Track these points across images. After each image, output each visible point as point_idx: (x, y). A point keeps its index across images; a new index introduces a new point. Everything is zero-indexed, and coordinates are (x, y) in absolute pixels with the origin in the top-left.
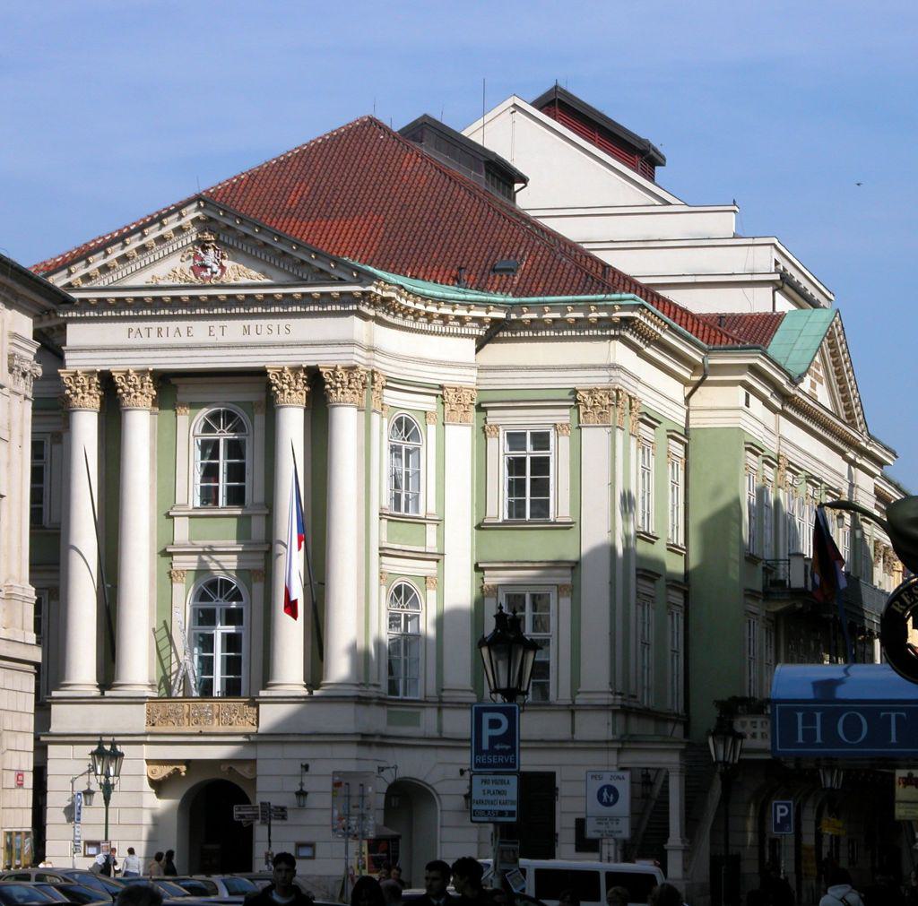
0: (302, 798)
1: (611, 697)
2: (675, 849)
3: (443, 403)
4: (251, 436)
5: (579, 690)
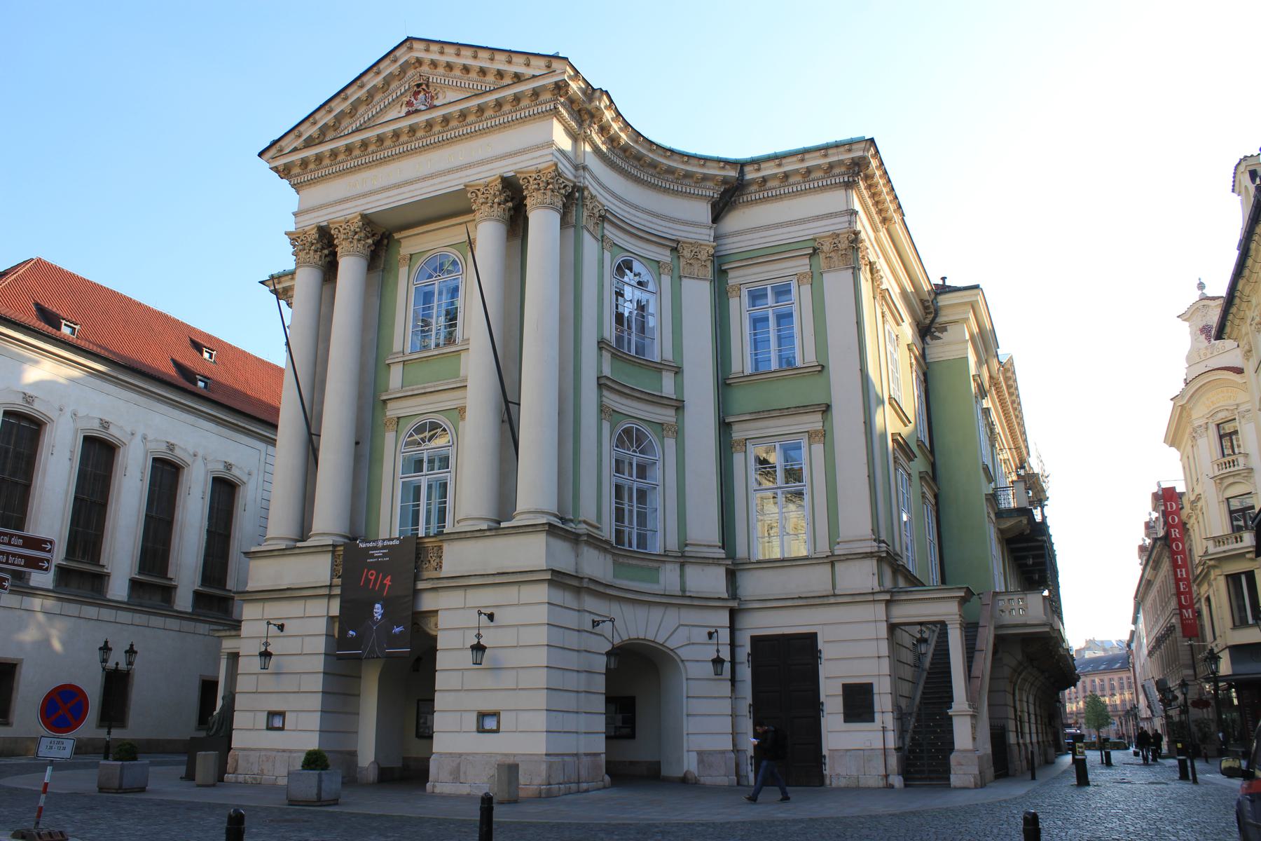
0: (480, 653)
1: (875, 544)
4: (464, 276)
5: (838, 540)
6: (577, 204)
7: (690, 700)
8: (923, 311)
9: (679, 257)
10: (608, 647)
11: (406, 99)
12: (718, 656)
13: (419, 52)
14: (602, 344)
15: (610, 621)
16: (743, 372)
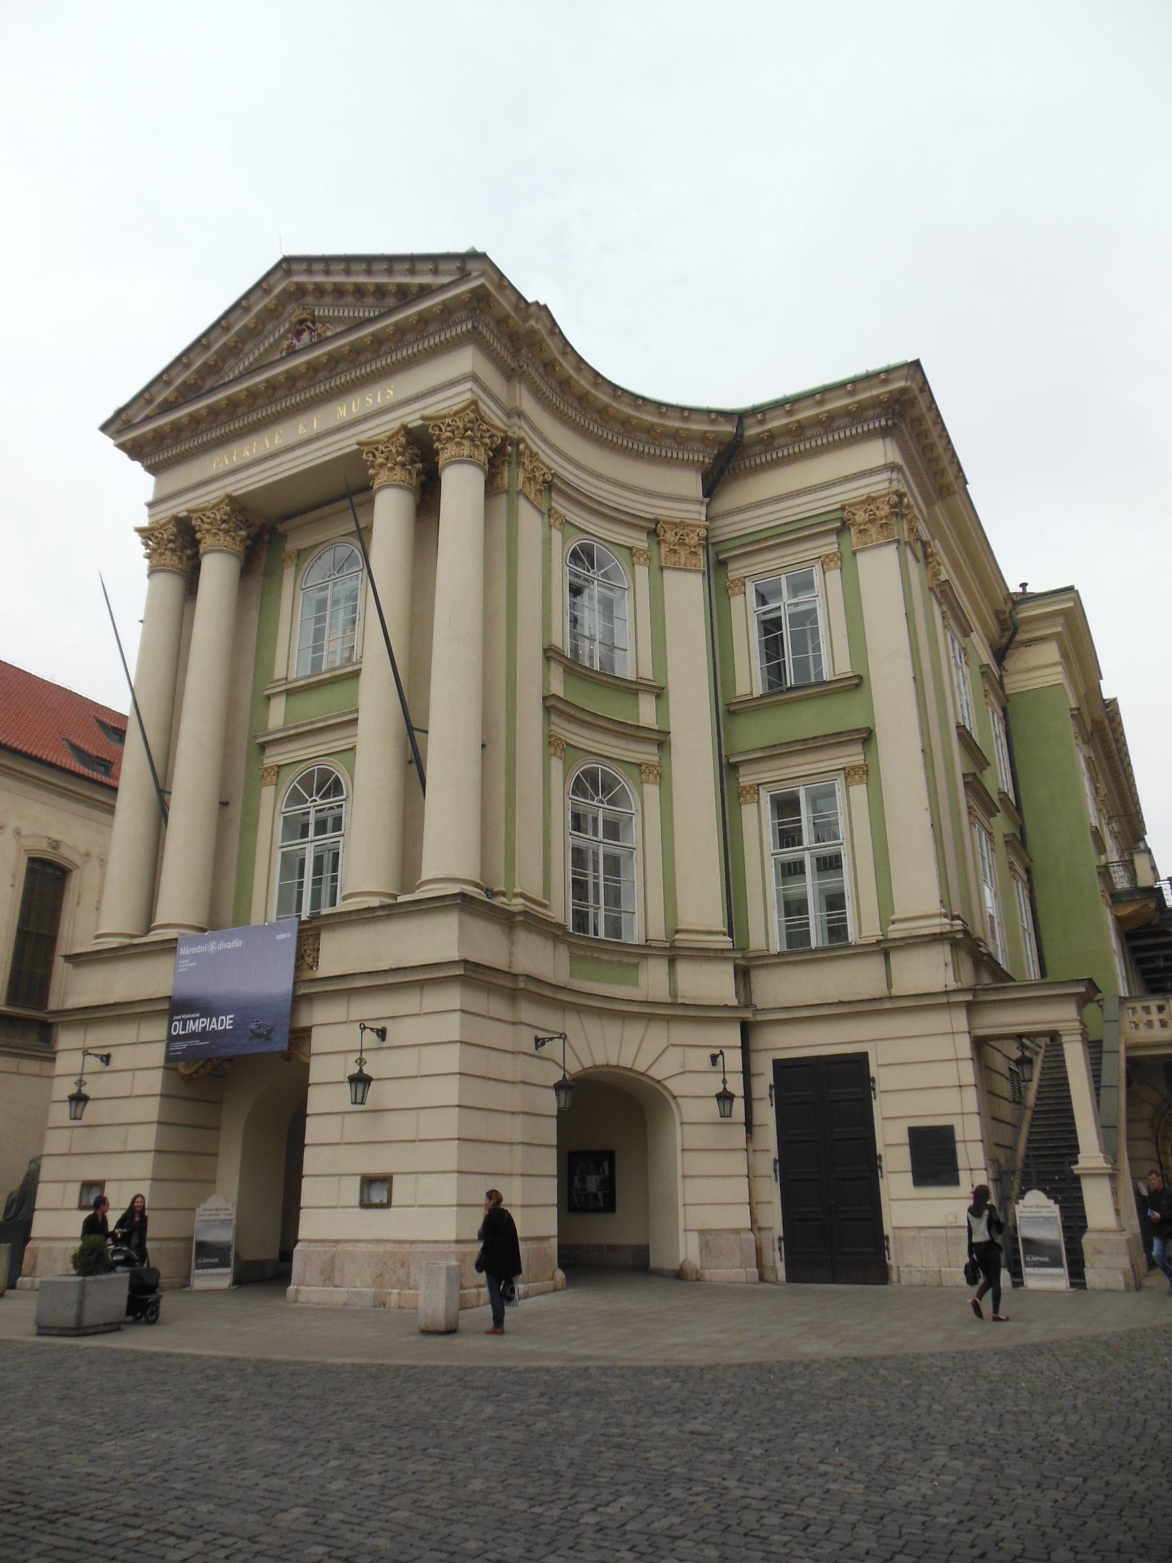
0: (360, 1087)
1: (946, 921)
2: (1094, 1174)
3: (659, 543)
5: (893, 917)
6: (510, 463)
7: (685, 1154)
8: (998, 627)
9: (659, 543)
10: (557, 1076)
11: (285, 344)
12: (725, 1088)
14: (550, 653)
15: (560, 1038)
16: (751, 694)
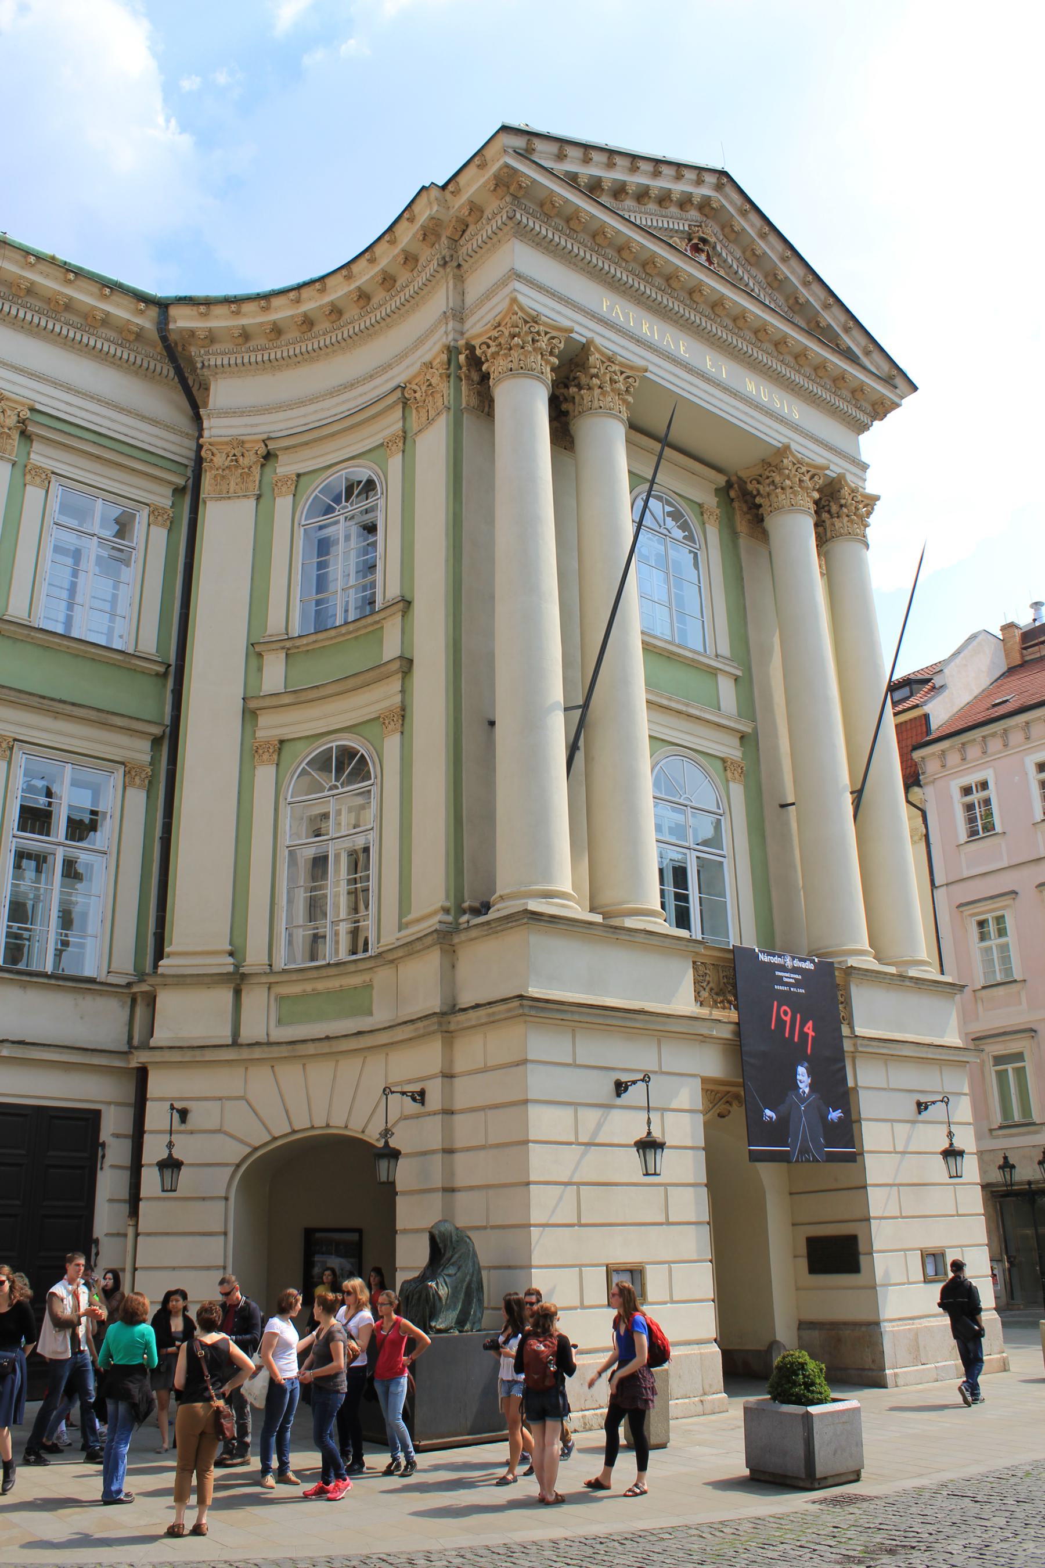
13: (729, 203)
